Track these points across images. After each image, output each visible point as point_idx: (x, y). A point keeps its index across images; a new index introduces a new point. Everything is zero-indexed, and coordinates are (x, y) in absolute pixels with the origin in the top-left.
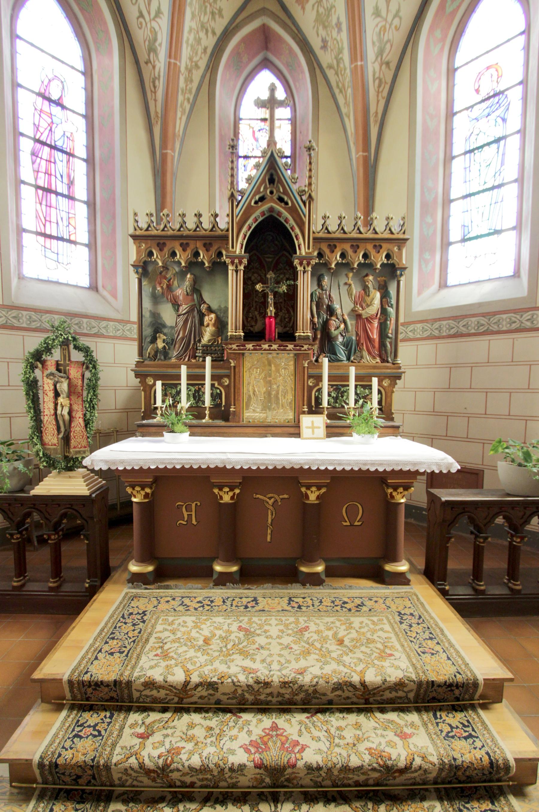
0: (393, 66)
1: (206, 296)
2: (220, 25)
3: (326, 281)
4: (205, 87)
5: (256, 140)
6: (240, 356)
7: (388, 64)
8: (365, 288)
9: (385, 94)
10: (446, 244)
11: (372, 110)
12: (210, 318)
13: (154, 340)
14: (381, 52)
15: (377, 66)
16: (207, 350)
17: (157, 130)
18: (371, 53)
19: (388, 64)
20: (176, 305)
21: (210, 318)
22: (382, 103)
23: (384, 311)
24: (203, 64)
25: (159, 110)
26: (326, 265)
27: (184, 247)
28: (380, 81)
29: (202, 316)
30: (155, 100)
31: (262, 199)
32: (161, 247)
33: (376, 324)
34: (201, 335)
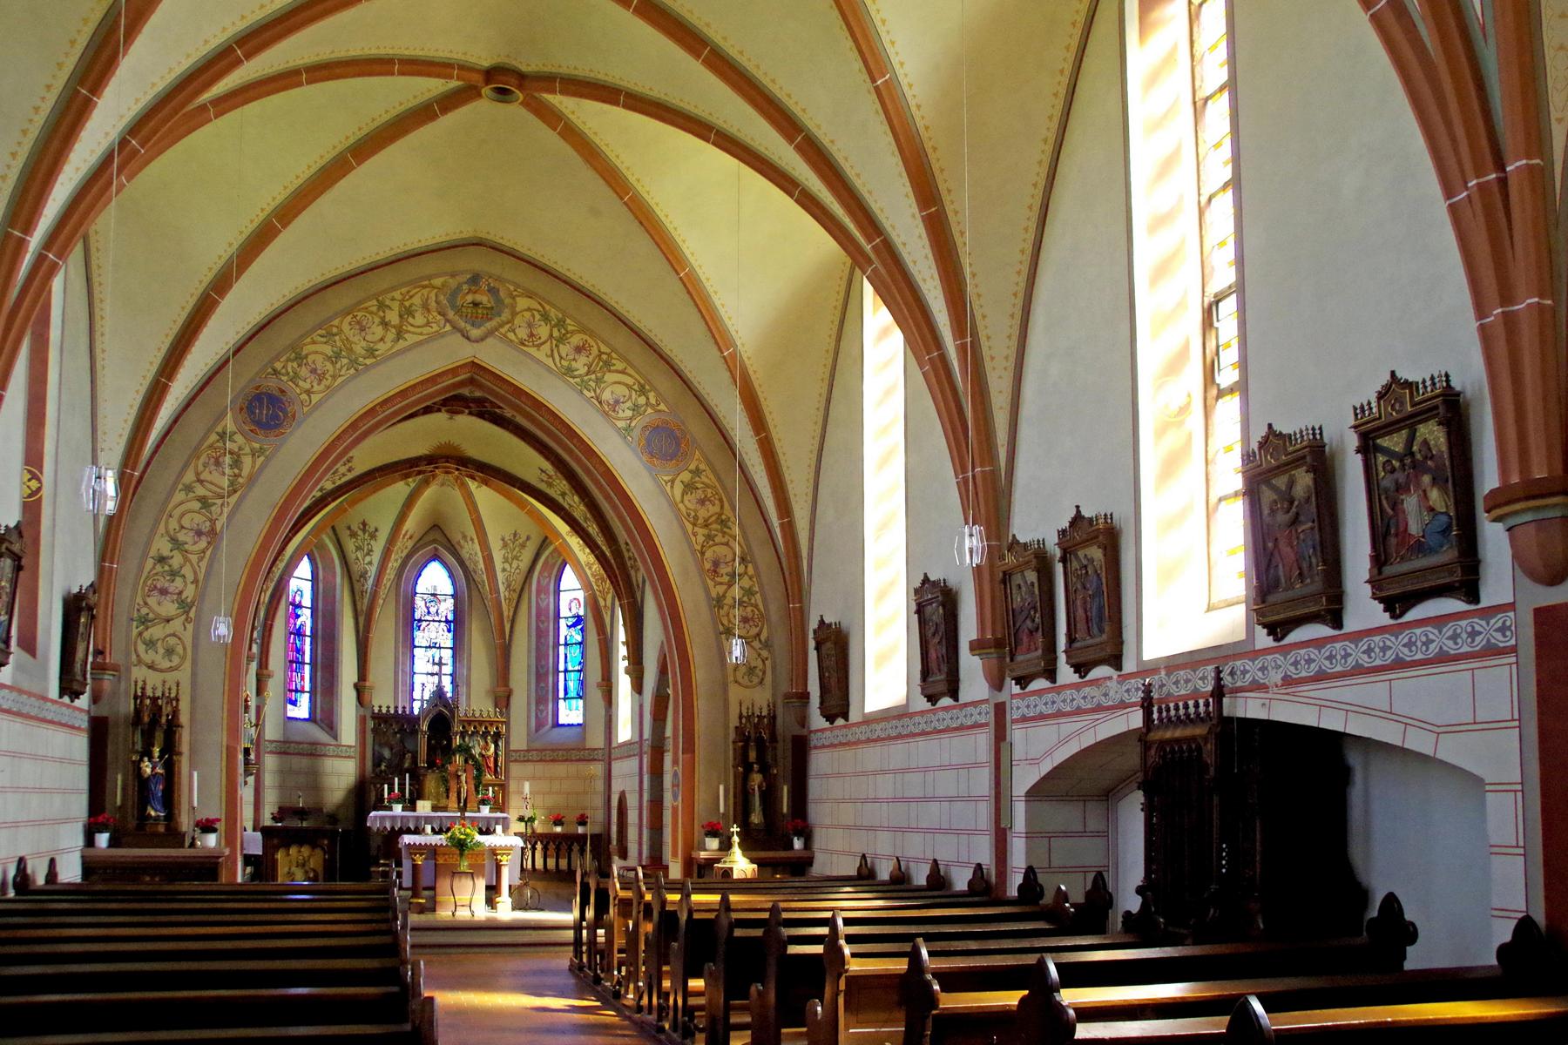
0: (518, 591)
1: (406, 745)
2: (406, 552)
3: (467, 739)
4: (394, 585)
5: (428, 608)
6: (425, 775)
7: (514, 590)
8: (486, 742)
9: (514, 605)
10: (556, 699)
11: (505, 614)
12: (408, 756)
13: (380, 765)
14: (509, 586)
15: (507, 593)
16: (407, 771)
17: (362, 620)
18: (502, 588)
19: (514, 590)
20: (391, 749)
21: (408, 756)
22: (512, 610)
23: (496, 753)
24: (392, 577)
25: (364, 608)
26: (467, 731)
27: (397, 723)
28: (510, 599)
29: (404, 754)
30: (362, 603)
31: (436, 705)
32: (386, 722)
33: (492, 759)
34: (404, 763)
